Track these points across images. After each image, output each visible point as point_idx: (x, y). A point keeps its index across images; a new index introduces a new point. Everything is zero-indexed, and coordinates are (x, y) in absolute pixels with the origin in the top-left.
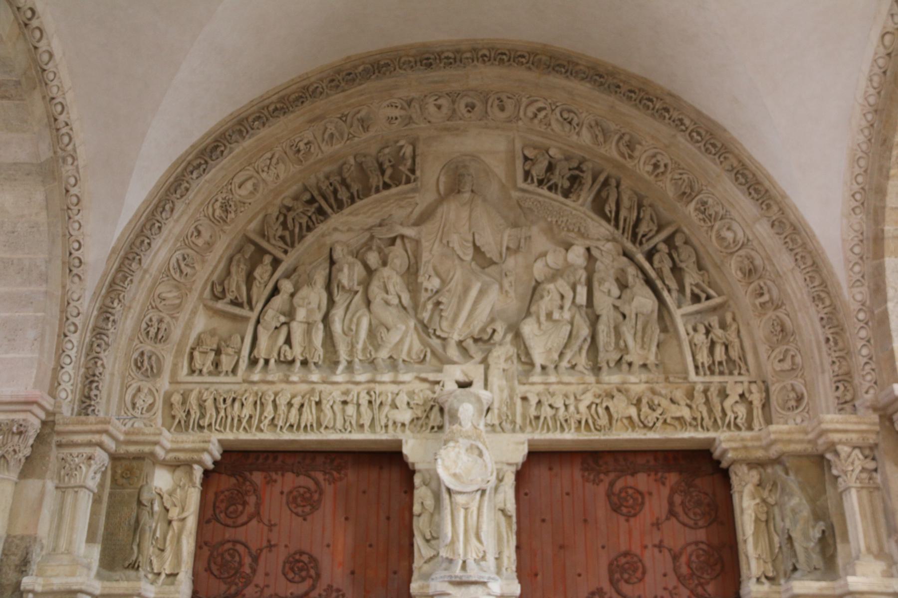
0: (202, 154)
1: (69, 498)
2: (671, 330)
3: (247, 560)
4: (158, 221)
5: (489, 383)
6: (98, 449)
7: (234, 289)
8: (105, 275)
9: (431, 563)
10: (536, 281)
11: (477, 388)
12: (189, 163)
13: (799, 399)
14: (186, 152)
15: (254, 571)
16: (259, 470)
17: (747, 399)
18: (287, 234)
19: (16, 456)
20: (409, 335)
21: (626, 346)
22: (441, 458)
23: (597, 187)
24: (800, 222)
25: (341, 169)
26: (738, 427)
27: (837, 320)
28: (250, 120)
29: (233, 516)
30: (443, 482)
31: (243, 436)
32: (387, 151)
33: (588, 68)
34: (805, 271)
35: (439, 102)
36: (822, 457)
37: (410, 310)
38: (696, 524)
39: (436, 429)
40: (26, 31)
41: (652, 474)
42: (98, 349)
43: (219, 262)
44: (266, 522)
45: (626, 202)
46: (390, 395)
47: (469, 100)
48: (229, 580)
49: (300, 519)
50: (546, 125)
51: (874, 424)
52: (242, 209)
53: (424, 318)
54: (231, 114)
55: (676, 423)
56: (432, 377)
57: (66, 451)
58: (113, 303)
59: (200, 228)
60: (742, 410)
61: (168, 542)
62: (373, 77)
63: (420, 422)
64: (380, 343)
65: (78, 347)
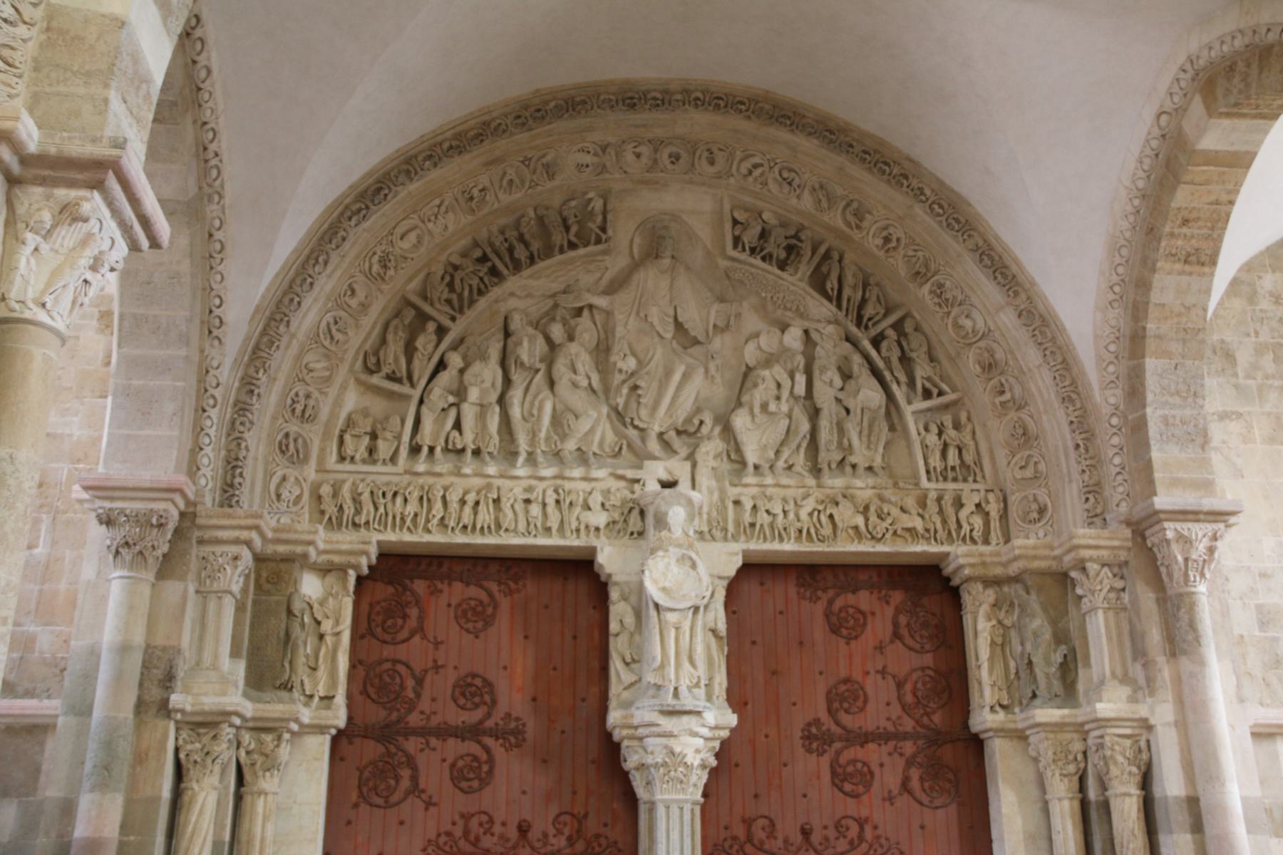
0: (361, 196)
1: (212, 606)
2: (899, 428)
3: (410, 683)
4: (310, 276)
5: (697, 483)
6: (245, 548)
7: (391, 361)
8: (248, 339)
9: (631, 690)
10: (747, 366)
11: (684, 486)
12: (347, 207)
13: (1042, 511)
14: (344, 193)
15: (418, 696)
16: (420, 578)
17: (983, 510)
18: (454, 297)
19: (155, 553)
20: (601, 424)
21: (850, 445)
23: (816, 259)
24: (1049, 313)
26: (973, 541)
27: (1088, 424)
28: (420, 158)
29: (391, 631)
30: (651, 596)
31: (407, 537)
32: (573, 203)
33: (817, 121)
34: (1055, 369)
35: (640, 149)
36: (1065, 575)
37: (602, 397)
38: (922, 648)
39: (635, 535)
40: (186, 42)
41: (876, 591)
42: (242, 428)
43: (373, 328)
44: (432, 640)
45: (849, 279)
46: (581, 493)
47: (674, 149)
48: (389, 705)
49: (471, 636)
50: (761, 184)
51: (1127, 539)
52: (404, 265)
53: (618, 405)
54: (397, 151)
55: (907, 535)
56: (630, 474)
57: (208, 549)
58: (257, 372)
59: (355, 286)
60: (978, 521)
61: (321, 660)
62: (566, 116)
63: (617, 527)
64: (567, 431)
65: (218, 424)
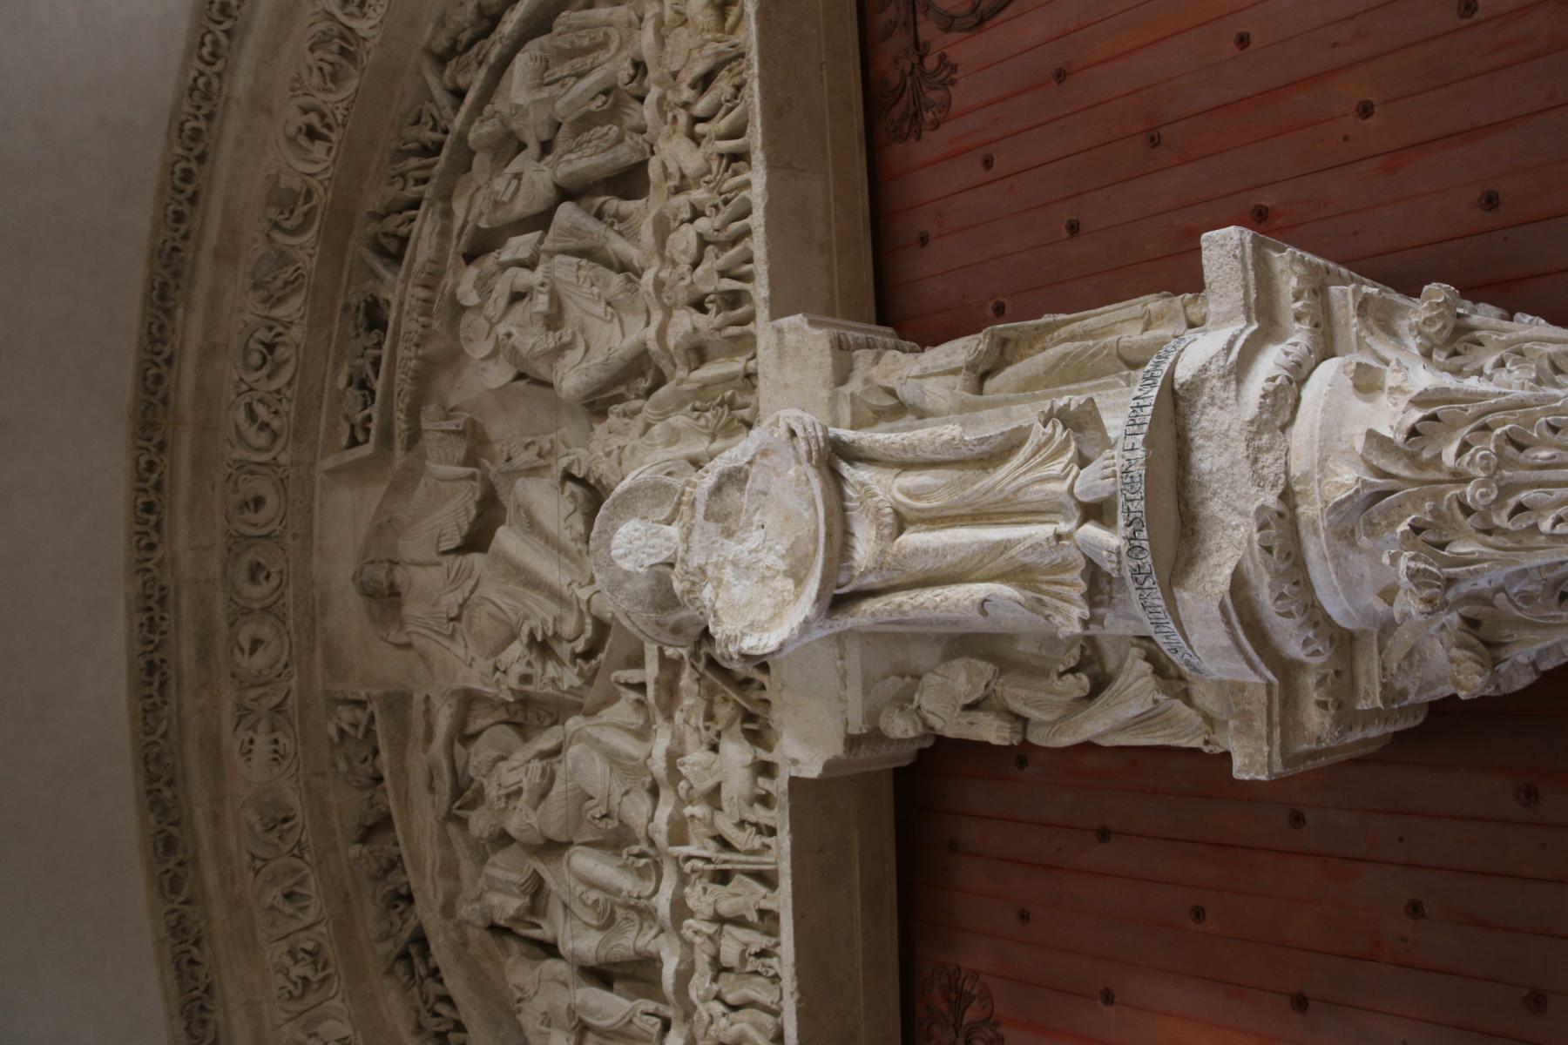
20: (595, 732)
21: (606, 92)
22: (743, 635)
23: (378, 264)
25: (375, 879)
45: (393, 192)
47: (242, 576)
